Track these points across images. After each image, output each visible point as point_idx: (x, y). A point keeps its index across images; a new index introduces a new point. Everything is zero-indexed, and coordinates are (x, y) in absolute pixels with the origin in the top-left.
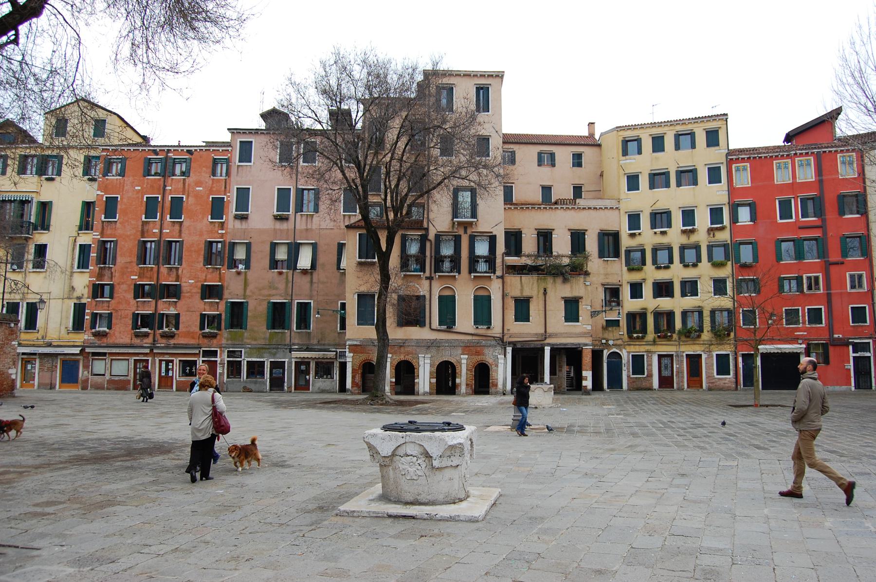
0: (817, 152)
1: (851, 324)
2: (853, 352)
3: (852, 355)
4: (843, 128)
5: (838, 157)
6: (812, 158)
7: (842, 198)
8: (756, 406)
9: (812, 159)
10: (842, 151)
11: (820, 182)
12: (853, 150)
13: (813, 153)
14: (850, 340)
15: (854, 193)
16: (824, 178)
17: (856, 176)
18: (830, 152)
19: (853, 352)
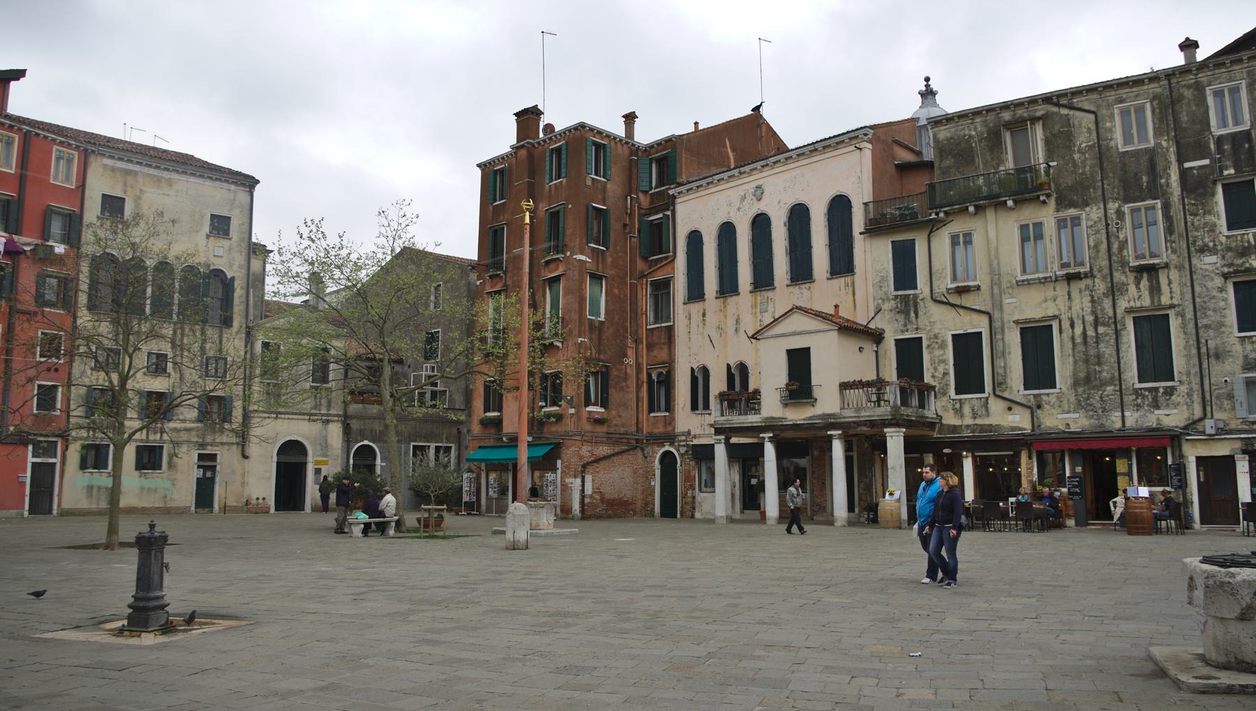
0: (27, 130)
1: (35, 412)
2: (34, 456)
3: (31, 459)
4: (21, 101)
5: (54, 149)
6: (17, 137)
7: (48, 213)
8: (108, 546)
9: (17, 139)
10: (61, 143)
11: (22, 179)
12: (77, 148)
13: (20, 130)
14: (30, 437)
15: (66, 211)
16: (28, 173)
17: (73, 187)
18: (45, 137)
19: (34, 456)
